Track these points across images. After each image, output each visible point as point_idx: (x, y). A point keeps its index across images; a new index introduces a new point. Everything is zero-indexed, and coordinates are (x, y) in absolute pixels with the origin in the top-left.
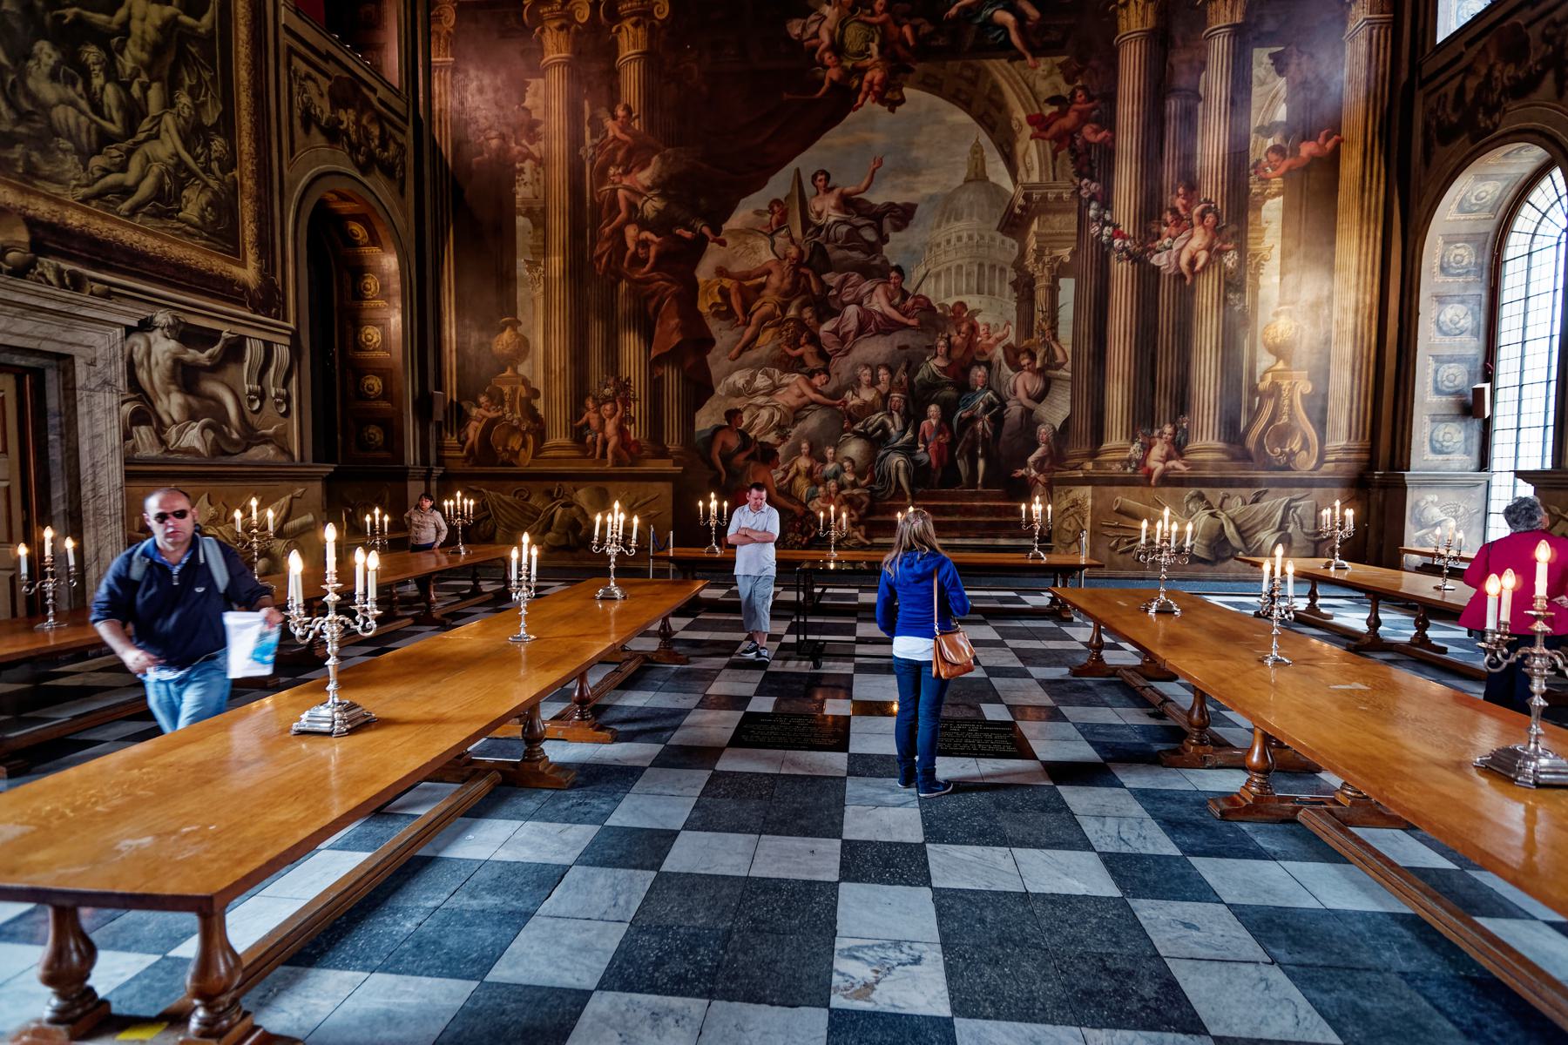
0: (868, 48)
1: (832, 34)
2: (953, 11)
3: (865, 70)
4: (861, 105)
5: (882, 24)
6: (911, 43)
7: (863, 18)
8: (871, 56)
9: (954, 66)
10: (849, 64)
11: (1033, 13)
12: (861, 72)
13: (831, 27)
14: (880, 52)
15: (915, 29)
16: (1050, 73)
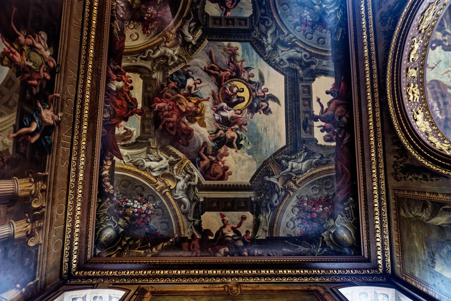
0: (31, 61)
1: (40, 49)
2: (40, 105)
3: (21, 54)
4: (3, 41)
5: (39, 73)
6: (30, 82)
7: (43, 66)
8: (27, 60)
9: (16, 98)
10: (25, 48)
11: (34, 140)
12: (21, 51)
13: (42, 51)
14: (28, 66)
15: (35, 86)
16: (4, 144)
